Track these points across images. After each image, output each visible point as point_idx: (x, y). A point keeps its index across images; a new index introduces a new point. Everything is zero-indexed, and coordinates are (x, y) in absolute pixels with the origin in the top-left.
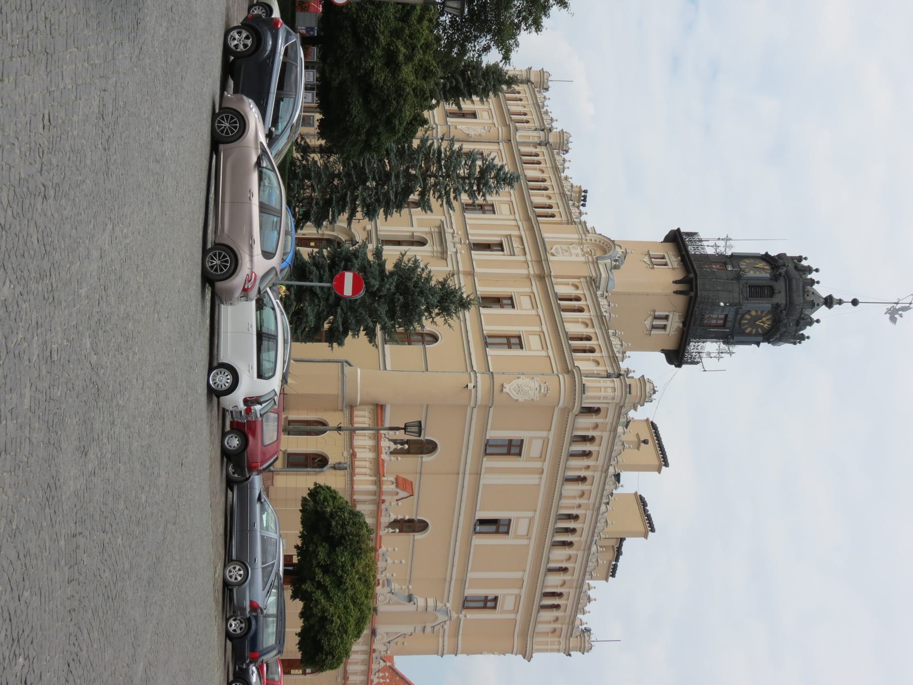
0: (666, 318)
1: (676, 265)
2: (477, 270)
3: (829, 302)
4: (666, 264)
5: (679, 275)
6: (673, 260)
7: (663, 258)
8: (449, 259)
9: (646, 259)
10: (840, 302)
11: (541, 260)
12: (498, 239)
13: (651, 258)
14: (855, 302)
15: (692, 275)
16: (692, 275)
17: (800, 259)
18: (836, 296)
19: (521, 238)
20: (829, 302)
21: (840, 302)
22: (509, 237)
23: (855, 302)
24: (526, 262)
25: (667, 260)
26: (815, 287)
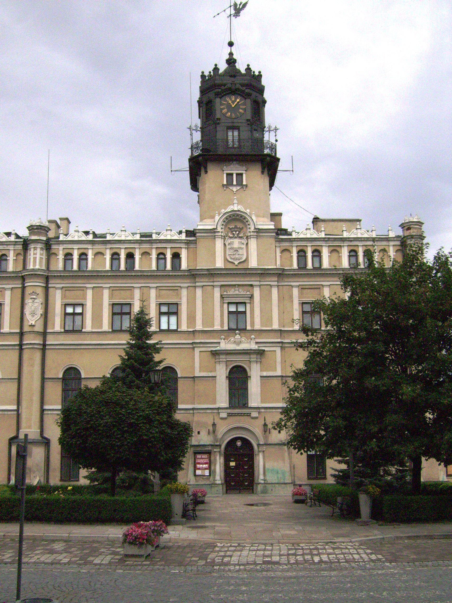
2: (276, 326)
3: (231, 61)
6: (235, 169)
8: (266, 349)
9: (235, 189)
10: (231, 54)
11: (263, 273)
12: (226, 306)
14: (231, 44)
18: (227, 57)
19: (222, 286)
20: (231, 61)
21: (231, 54)
22: (222, 297)
24: (260, 286)
25: (235, 172)
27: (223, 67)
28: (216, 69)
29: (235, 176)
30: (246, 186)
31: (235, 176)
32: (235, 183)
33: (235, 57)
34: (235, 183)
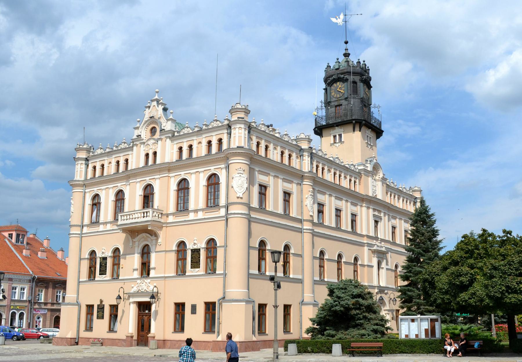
0: (367, 136)
1: (342, 130)
3: (347, 55)
4: (340, 136)
5: (352, 129)
6: (337, 131)
7: (335, 137)
9: (337, 145)
10: (346, 50)
13: (335, 142)
14: (346, 43)
15: (354, 122)
16: (354, 122)
17: (329, 66)
18: (344, 52)
20: (347, 55)
23: (346, 43)
26: (340, 60)
27: (342, 59)
28: (329, 66)
29: (337, 136)
30: (343, 142)
31: (337, 136)
32: (337, 141)
33: (349, 52)
34: (337, 141)
